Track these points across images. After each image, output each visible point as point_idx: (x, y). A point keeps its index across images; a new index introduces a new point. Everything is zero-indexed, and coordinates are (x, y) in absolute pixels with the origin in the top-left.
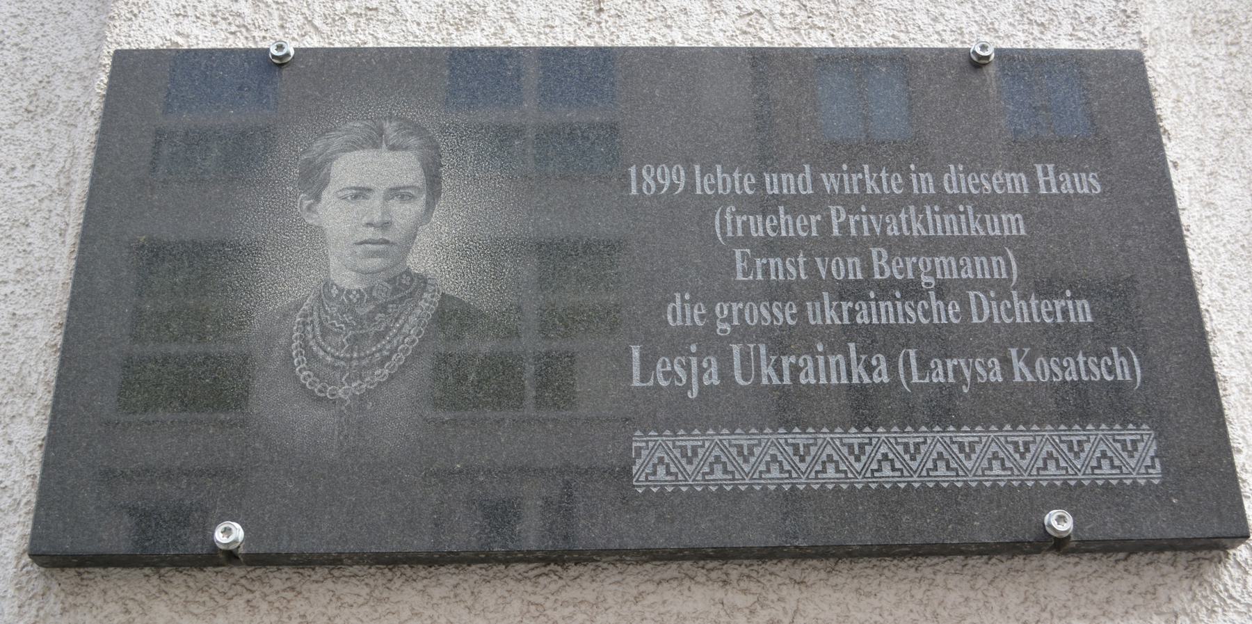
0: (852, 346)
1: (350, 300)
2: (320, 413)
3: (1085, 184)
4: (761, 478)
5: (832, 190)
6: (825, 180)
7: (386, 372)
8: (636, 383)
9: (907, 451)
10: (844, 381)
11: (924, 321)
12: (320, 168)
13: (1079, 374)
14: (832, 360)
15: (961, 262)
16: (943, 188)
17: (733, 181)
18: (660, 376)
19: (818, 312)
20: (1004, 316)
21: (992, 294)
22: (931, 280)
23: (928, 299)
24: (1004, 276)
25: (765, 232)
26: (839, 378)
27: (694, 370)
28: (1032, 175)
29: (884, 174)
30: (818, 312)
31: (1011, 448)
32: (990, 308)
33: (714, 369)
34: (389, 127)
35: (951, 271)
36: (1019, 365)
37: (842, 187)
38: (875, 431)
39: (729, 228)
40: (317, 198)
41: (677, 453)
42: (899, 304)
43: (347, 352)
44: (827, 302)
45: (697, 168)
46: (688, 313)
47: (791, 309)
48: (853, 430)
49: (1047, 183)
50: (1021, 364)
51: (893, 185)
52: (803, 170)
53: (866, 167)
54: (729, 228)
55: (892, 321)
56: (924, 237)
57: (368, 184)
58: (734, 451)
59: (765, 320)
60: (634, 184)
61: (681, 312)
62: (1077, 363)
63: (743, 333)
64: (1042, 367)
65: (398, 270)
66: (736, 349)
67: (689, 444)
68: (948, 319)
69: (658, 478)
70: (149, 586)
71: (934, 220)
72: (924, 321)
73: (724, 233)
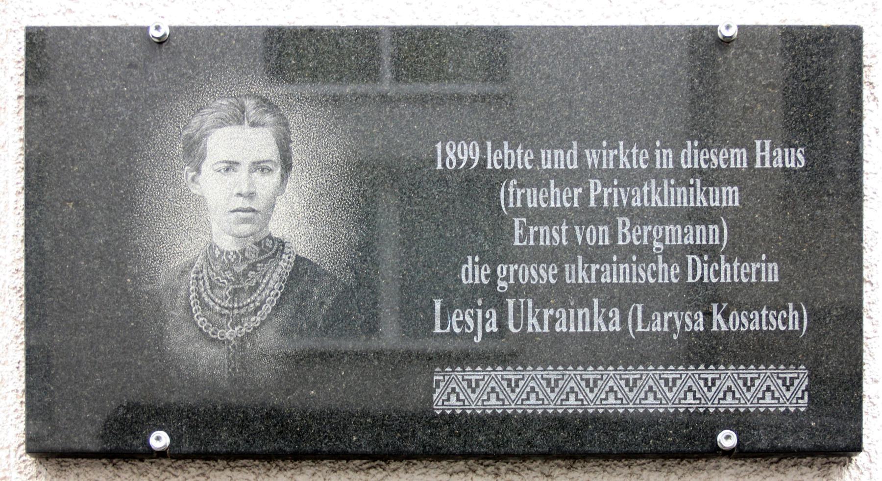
0: (596, 301)
1: (229, 260)
2: (214, 351)
3: (793, 158)
4: (522, 404)
5: (593, 165)
6: (588, 156)
7: (259, 319)
8: (438, 330)
9: (627, 385)
10: (588, 329)
11: (651, 280)
12: (198, 143)
13: (761, 325)
14: (580, 313)
15: (686, 230)
16: (679, 163)
19: (573, 273)
20: (712, 276)
21: (706, 258)
23: (656, 262)
24: (717, 242)
25: (538, 203)
26: (584, 328)
27: (480, 320)
28: (751, 150)
29: (634, 151)
30: (573, 273)
31: (702, 383)
32: (703, 269)
33: (494, 320)
34: (250, 104)
35: (677, 237)
36: (717, 317)
37: (600, 163)
38: (606, 370)
39: (511, 199)
40: (198, 170)
41: (465, 384)
44: (580, 264)
45: (489, 144)
47: (554, 270)
48: (591, 368)
49: (763, 158)
50: (719, 316)
52: (571, 147)
53: (621, 143)
54: (511, 199)
55: (628, 281)
56: (660, 208)
57: (235, 159)
58: (505, 383)
59: (534, 279)
60: (439, 159)
61: (473, 272)
62: (760, 316)
63: (517, 290)
66: (511, 302)
67: (473, 378)
68: (669, 279)
69: (450, 403)
70: (106, 472)
71: (669, 193)
72: (651, 280)
73: (507, 204)
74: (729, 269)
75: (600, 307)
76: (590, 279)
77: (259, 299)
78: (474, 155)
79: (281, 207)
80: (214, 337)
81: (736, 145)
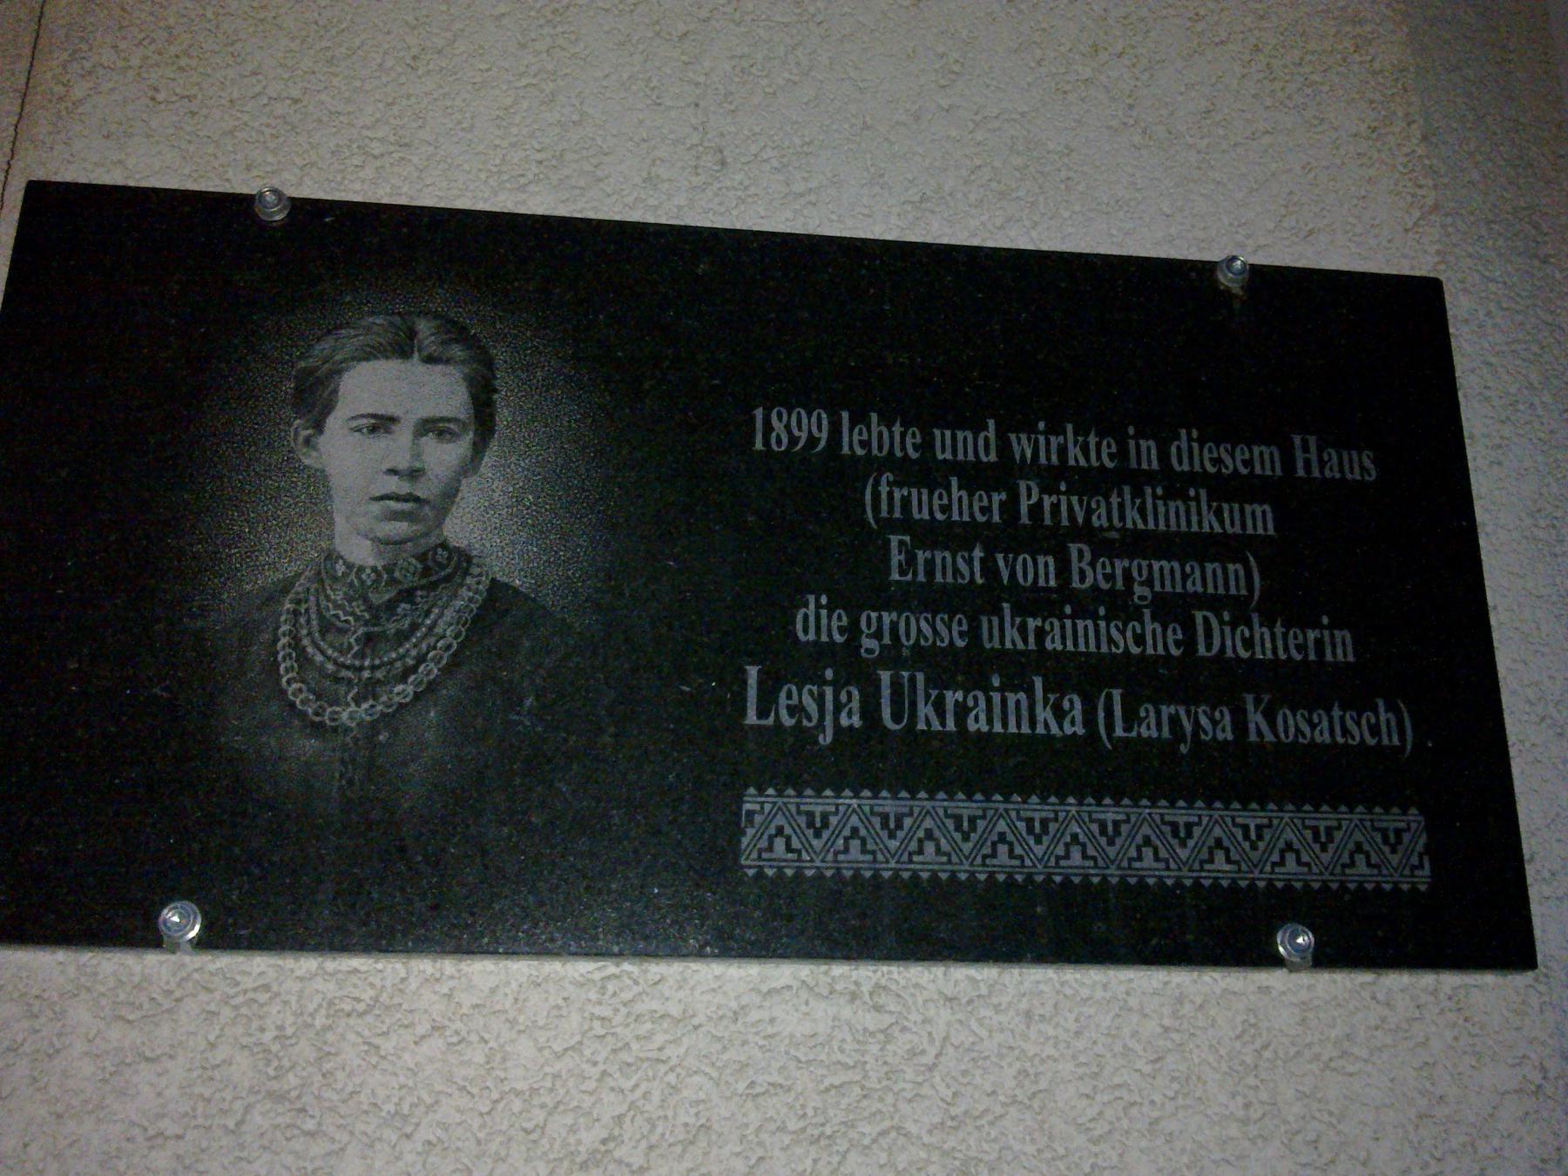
0: (1038, 683)
1: (363, 582)
4: (911, 861)
6: (1015, 444)
7: (410, 689)
8: (752, 718)
9: (1103, 831)
10: (1026, 729)
11: (1135, 650)
17: (892, 438)
18: (783, 713)
21: (1226, 616)
22: (1146, 592)
24: (1244, 592)
26: (1019, 726)
27: (829, 706)
33: (855, 704)
34: (424, 327)
36: (1255, 718)
38: (1062, 803)
39: (884, 507)
40: (319, 426)
41: (802, 821)
42: (1102, 624)
43: (355, 656)
44: (1008, 619)
45: (845, 415)
46: (824, 621)
47: (960, 624)
51: (1103, 454)
52: (986, 428)
53: (1070, 427)
54: (884, 507)
57: (391, 410)
58: (876, 821)
59: (926, 639)
63: (892, 656)
64: (1285, 722)
65: (433, 540)
66: (885, 676)
67: (818, 810)
69: (774, 856)
72: (1135, 650)
74: (1267, 637)
75: (1046, 691)
76: (1025, 641)
77: (414, 653)
78: (820, 428)
79: (470, 495)
80: (317, 719)
81: (1261, 442)
